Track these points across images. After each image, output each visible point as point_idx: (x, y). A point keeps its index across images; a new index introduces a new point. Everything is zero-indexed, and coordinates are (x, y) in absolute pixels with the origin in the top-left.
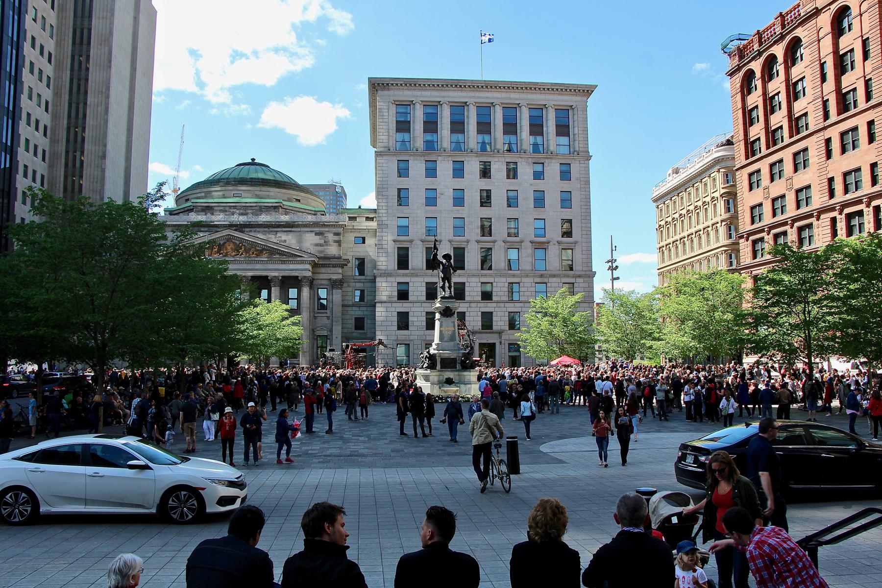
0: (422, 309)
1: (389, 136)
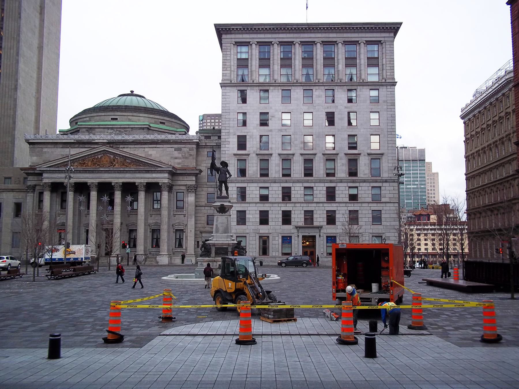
0: (256, 208)
1: (231, 71)
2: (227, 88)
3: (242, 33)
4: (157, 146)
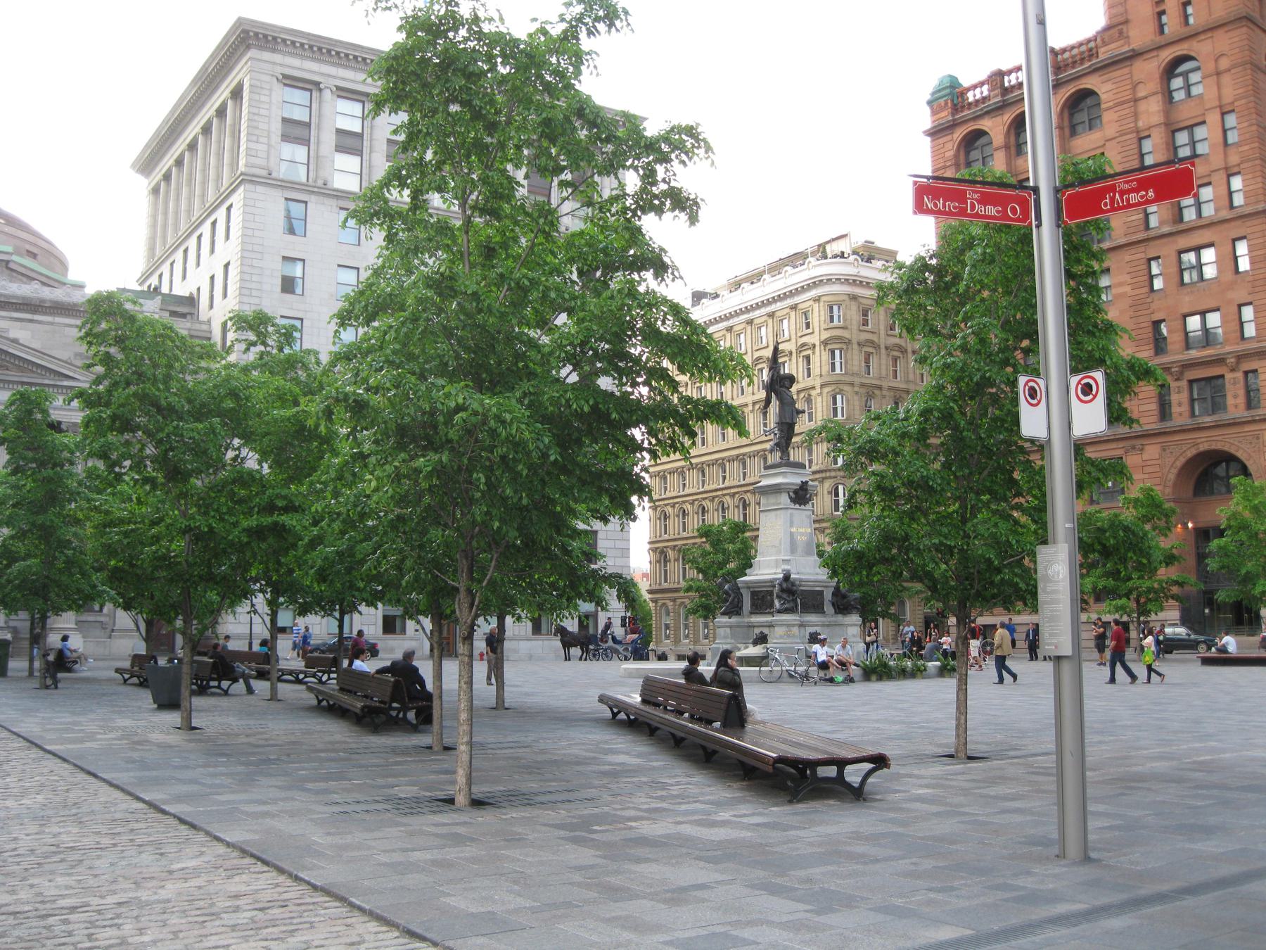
1: (269, 145)
2: (260, 189)
3: (303, 57)
4: (37, 317)
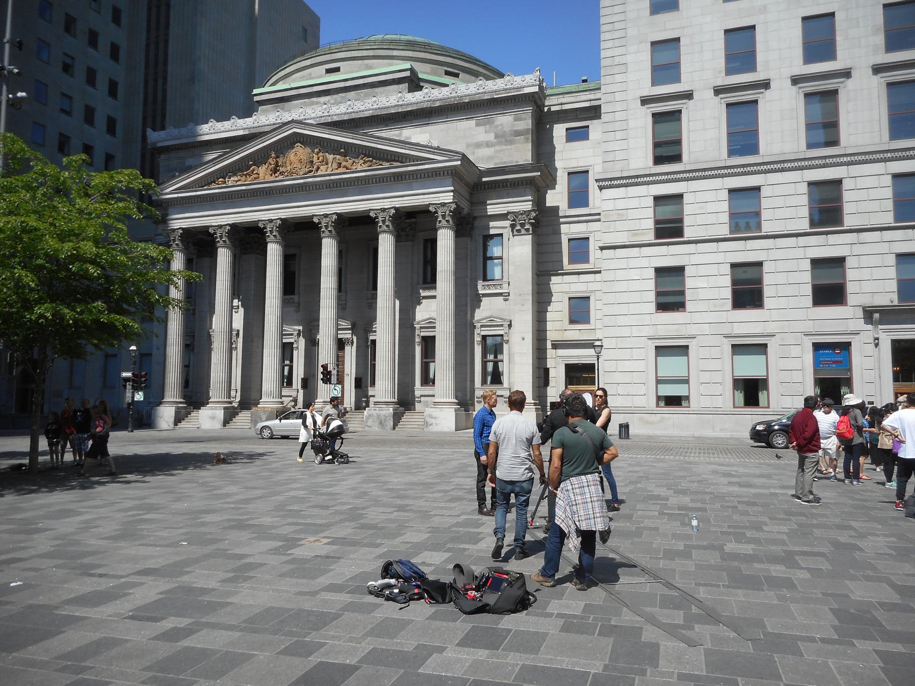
0: (720, 258)
